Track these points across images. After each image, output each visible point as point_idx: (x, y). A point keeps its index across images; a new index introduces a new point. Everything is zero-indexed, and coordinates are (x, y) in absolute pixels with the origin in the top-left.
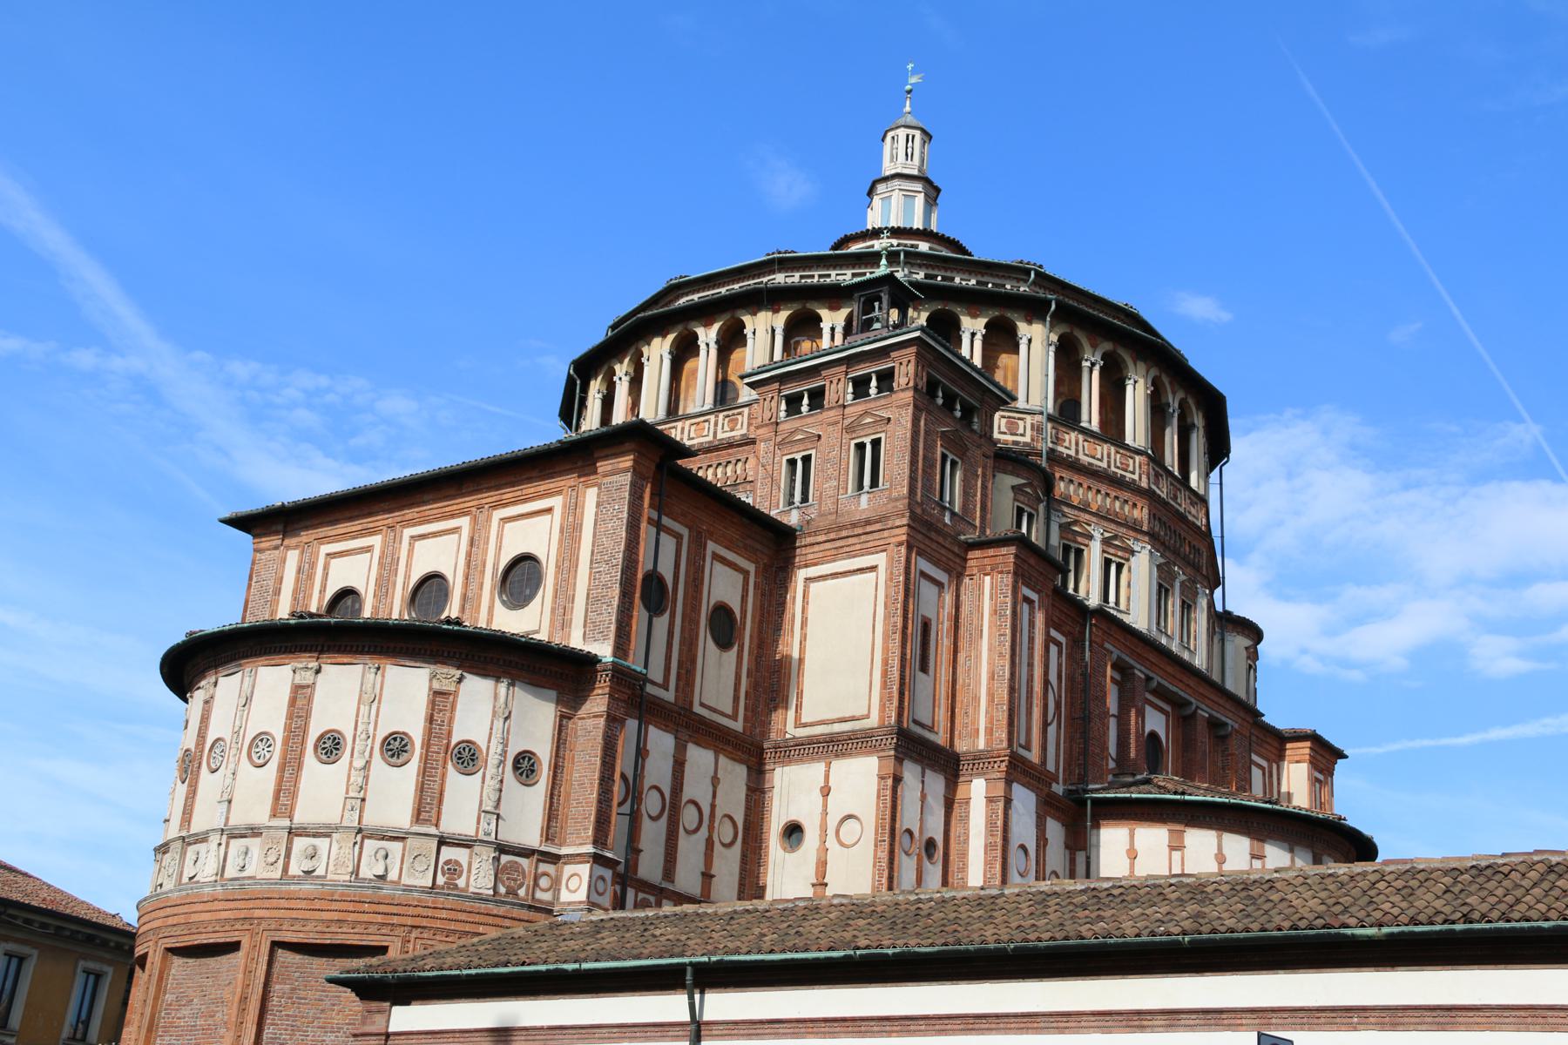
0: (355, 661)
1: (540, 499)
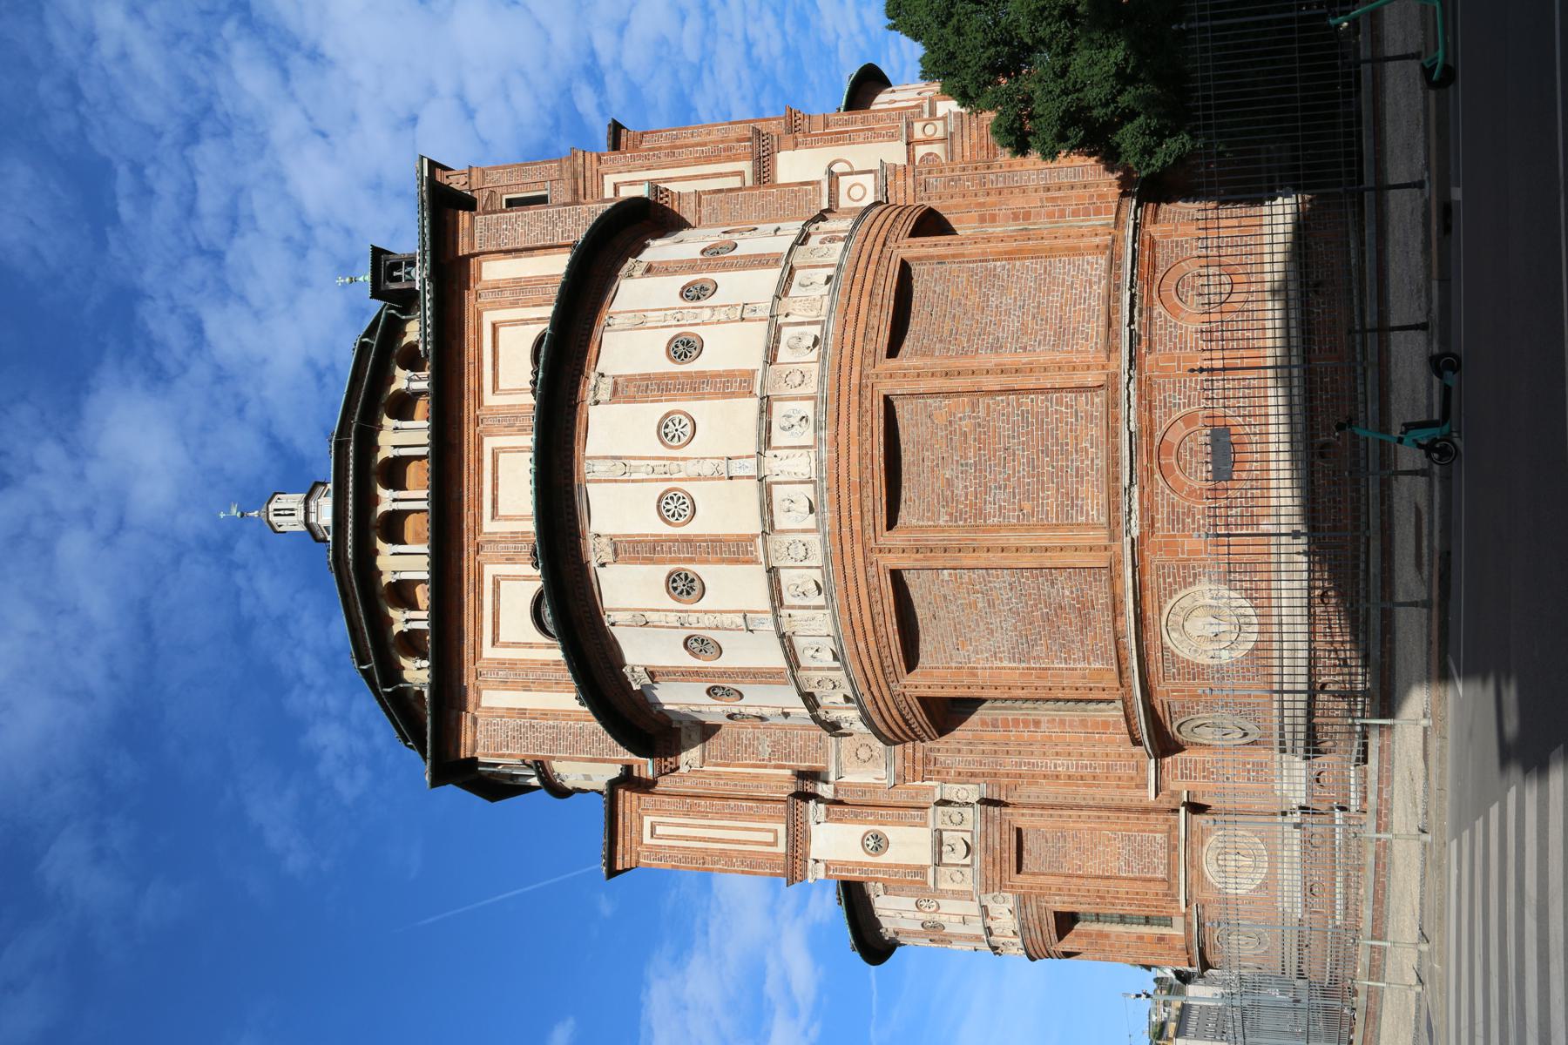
1: (482, 341)
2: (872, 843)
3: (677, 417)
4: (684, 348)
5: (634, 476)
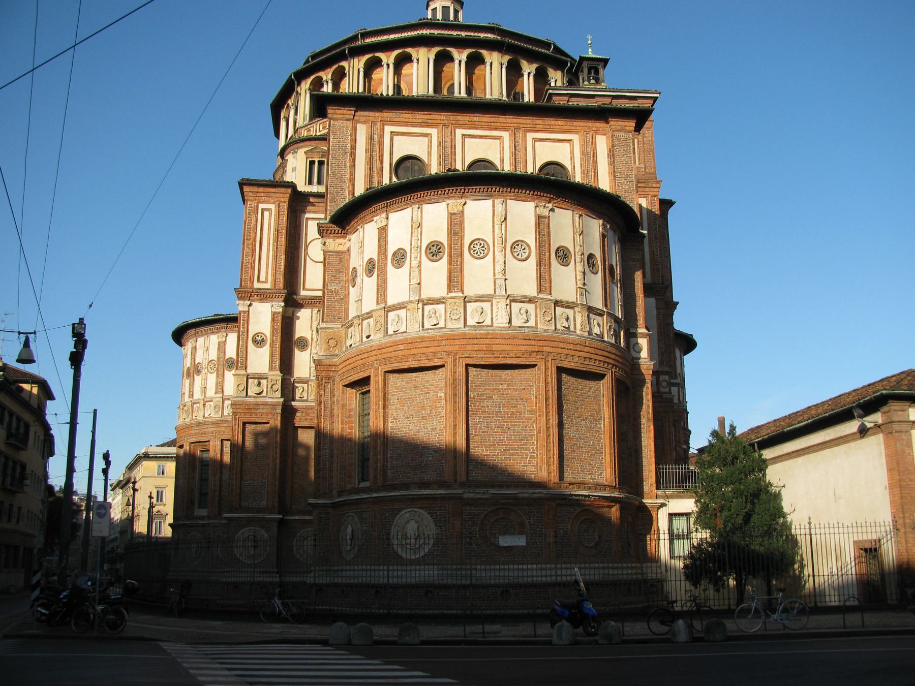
0: (568, 208)
2: (259, 338)
3: (527, 251)
4: (563, 255)
5: (496, 226)
